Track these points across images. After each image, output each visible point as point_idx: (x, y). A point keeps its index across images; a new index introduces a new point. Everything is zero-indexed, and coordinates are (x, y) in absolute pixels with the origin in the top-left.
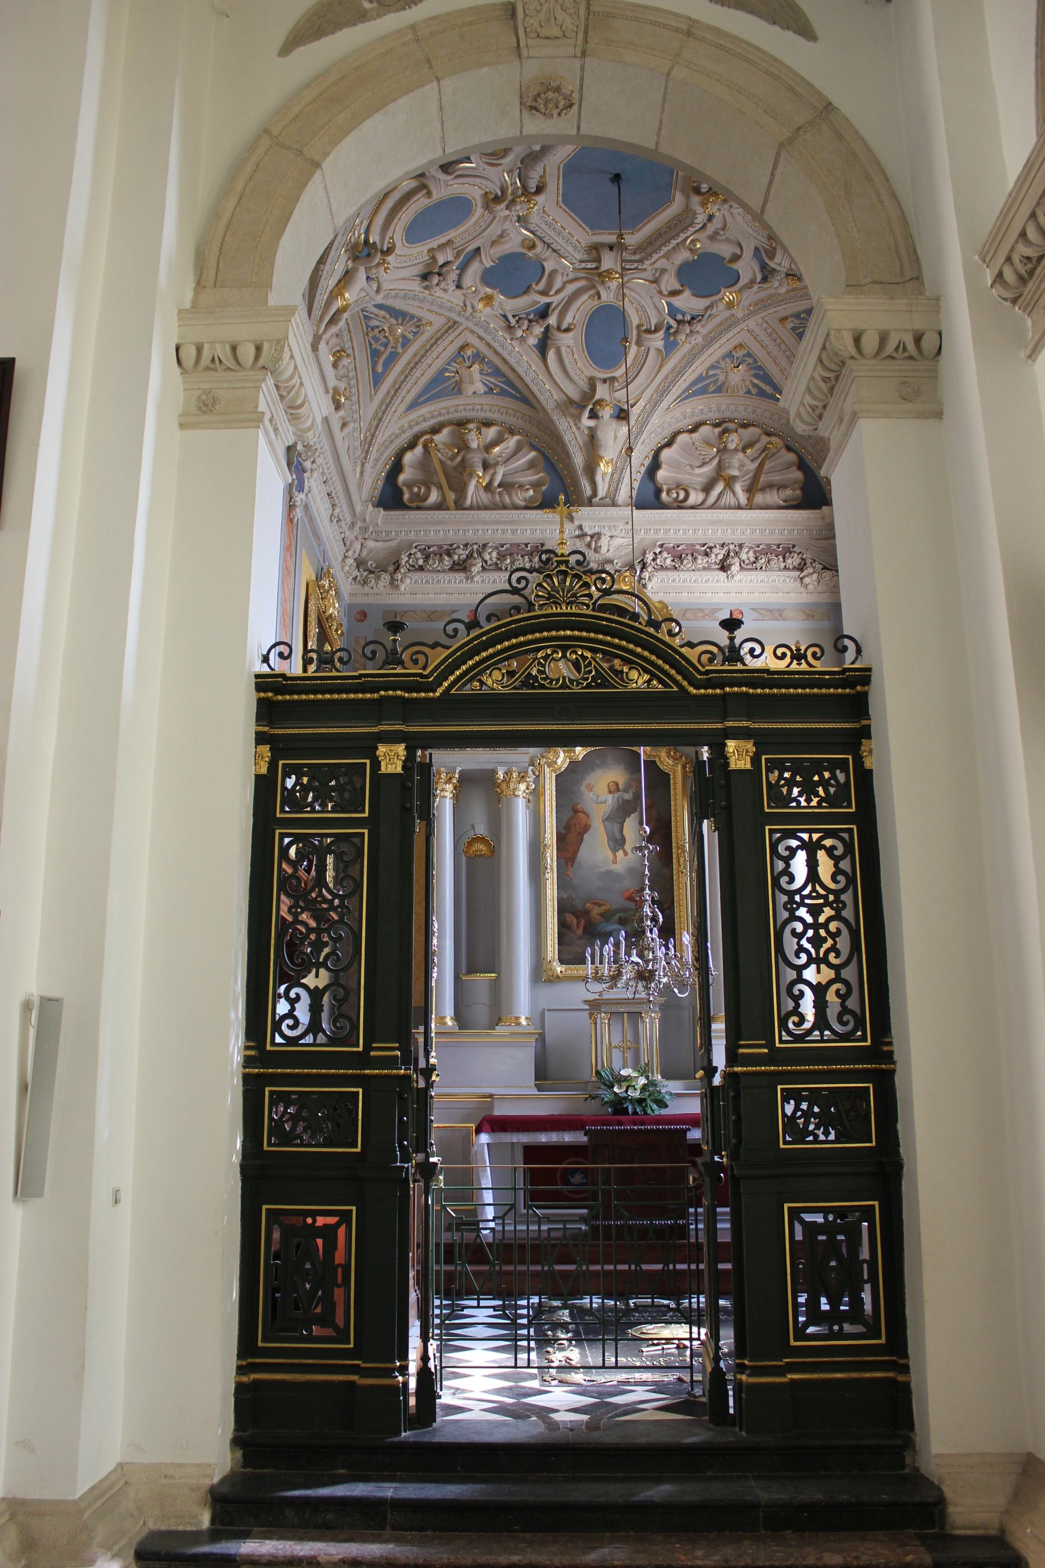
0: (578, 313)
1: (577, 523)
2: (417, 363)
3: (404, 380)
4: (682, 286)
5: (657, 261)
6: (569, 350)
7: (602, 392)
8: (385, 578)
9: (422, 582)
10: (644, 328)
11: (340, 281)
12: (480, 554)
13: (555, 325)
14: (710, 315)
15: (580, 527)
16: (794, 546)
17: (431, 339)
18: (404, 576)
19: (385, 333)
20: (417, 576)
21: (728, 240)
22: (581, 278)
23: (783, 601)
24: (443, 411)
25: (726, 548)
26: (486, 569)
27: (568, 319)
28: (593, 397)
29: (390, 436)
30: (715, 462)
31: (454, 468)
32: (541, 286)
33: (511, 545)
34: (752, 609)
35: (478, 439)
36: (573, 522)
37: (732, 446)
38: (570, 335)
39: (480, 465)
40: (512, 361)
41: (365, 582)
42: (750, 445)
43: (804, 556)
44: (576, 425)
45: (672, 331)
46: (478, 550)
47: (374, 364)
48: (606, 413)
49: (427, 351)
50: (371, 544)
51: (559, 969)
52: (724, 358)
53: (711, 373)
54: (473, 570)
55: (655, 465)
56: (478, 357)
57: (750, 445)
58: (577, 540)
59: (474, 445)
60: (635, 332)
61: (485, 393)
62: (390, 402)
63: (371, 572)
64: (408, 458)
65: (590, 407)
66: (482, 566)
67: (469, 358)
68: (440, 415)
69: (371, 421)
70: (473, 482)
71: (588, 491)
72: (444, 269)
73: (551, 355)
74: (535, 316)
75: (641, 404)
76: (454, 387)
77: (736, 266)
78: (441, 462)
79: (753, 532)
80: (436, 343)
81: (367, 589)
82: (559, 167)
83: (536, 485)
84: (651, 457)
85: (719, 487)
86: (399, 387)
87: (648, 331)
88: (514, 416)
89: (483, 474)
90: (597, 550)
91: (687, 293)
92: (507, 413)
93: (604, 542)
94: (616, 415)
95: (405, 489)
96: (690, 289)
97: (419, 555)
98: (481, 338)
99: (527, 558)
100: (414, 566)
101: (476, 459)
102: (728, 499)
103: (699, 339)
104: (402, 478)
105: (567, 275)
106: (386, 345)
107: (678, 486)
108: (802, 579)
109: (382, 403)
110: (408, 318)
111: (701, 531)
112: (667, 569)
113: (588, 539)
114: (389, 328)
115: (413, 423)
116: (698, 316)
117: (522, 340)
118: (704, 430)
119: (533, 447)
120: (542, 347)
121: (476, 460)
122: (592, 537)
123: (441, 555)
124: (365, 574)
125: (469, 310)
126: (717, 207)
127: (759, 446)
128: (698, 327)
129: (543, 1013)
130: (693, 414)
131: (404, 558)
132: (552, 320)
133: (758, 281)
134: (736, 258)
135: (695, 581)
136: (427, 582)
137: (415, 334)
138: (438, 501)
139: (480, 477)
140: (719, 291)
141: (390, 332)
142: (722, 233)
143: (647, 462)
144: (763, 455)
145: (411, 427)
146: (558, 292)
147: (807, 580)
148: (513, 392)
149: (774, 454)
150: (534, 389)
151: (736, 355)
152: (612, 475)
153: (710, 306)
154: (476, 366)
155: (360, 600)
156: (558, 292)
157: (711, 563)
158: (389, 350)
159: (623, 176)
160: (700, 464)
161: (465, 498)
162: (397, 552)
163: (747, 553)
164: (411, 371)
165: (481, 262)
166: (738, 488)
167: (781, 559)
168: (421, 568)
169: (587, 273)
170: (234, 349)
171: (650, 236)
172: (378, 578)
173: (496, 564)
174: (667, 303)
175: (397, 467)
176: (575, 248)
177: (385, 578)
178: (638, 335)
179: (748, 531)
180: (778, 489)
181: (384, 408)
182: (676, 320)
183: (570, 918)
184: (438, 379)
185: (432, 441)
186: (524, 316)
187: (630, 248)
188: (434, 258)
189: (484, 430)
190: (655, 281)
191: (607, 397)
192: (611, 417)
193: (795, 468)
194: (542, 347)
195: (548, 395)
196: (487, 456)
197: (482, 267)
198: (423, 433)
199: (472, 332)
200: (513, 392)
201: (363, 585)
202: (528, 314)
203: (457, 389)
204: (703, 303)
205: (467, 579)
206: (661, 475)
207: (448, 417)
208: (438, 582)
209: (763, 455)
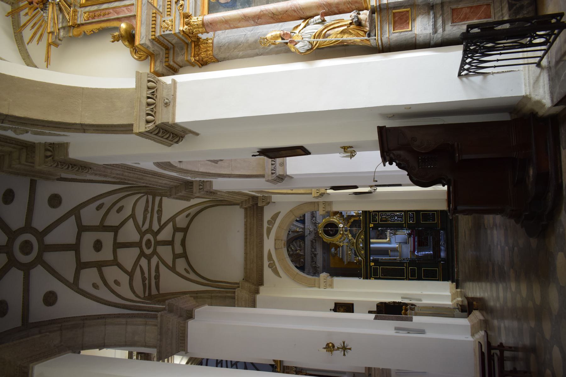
12: (313, 252)
18: (317, 265)
20: (317, 263)
50: (311, 272)
51: (388, 239)
71: (301, 233)
83: (300, 242)
90: (312, 231)
93: (311, 230)
95: (300, 265)
104: (298, 266)
119: (293, 242)
121: (295, 253)
129: (396, 243)
168: (315, 262)
170: (324, 282)
172: (318, 270)
183: (379, 238)
189: (289, 251)
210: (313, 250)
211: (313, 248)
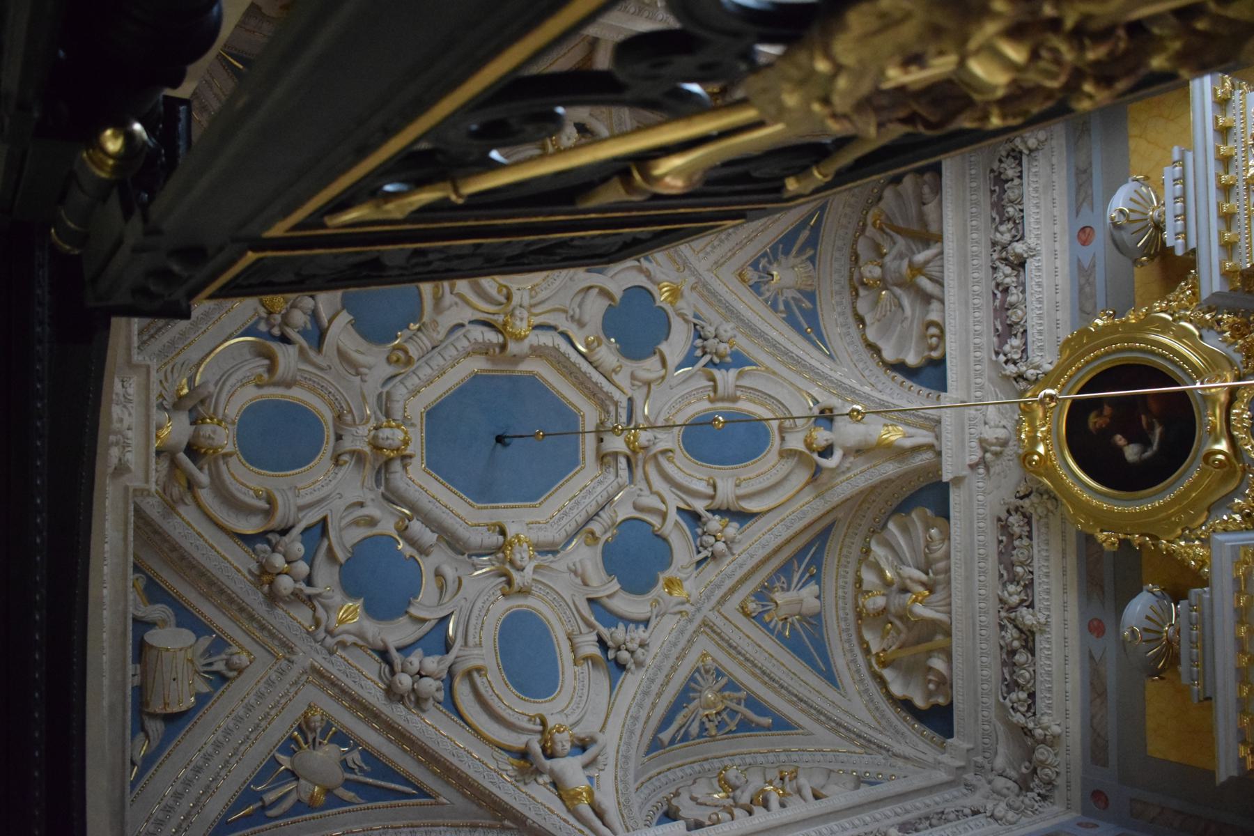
0: (695, 476)
1: (966, 472)
2: (764, 673)
3: (786, 689)
4: (655, 353)
5: (621, 388)
6: (743, 484)
7: (795, 442)
9: (1049, 698)
10: (712, 394)
11: (560, 797)
12: (1012, 609)
13: (706, 503)
14: (696, 316)
15: (973, 467)
16: (992, 171)
17: (730, 654)
18: (1037, 724)
19: (711, 715)
20: (1041, 705)
21: (580, 306)
22: (645, 473)
23: (1064, 173)
24: (844, 636)
25: (998, 263)
26: (1033, 601)
27: (702, 487)
28: (801, 453)
29: (869, 710)
30: (898, 291)
31: (910, 629)
32: (655, 521)
33: (1000, 563)
34: (1077, 216)
35: (873, 595)
36: (963, 478)
37: (877, 271)
38: (720, 484)
39: (902, 596)
40: (761, 554)
41: (1050, 783)
42: (877, 248)
43: (1004, 153)
44: (843, 473)
45: (716, 360)
46: (1007, 611)
47: (760, 727)
48: (822, 436)
49: (747, 660)
50: (1000, 762)
52: (760, 294)
53: (782, 307)
54: (1028, 622)
55: (900, 368)
56: (763, 594)
57: (877, 248)
58: (992, 471)
59: (880, 601)
60: (719, 405)
61: (818, 583)
62: (815, 709)
63: (1034, 771)
64: (897, 689)
65: (815, 456)
66: (1028, 607)
67: (763, 606)
68: (849, 641)
69: (841, 737)
70: (919, 609)
71: (925, 458)
72: (610, 643)
73: (751, 506)
74: (699, 527)
75: (815, 391)
76: (809, 623)
77: (618, 295)
79: (976, 229)
80: (735, 648)
81: (1060, 782)
82: (479, 508)
84: (894, 374)
85: (924, 282)
86: (796, 696)
87: (715, 389)
88: (850, 547)
89: (914, 594)
90: (1004, 444)
91: (664, 347)
92: (846, 557)
94: (828, 423)
95: (933, 700)
96: (659, 343)
97: (1013, 696)
98: (732, 590)
99: (1017, 543)
100: (1029, 707)
101: (896, 602)
102: (932, 269)
103: (727, 329)
104: (920, 702)
105: (641, 490)
106: (733, 713)
107: (924, 337)
108: (1031, 151)
109: (818, 720)
110: (693, 685)
111: (976, 301)
112: (1025, 344)
113: (988, 455)
114: (704, 709)
115: (856, 677)
116: (695, 329)
117: (729, 543)
118: (862, 307)
119: (884, 526)
120: (743, 517)
121: (898, 601)
122: (985, 451)
123: (1014, 664)
124: (1036, 780)
125: (687, 607)
126: (518, 323)
127: (879, 238)
128: (710, 330)
130: (844, 325)
131: (1018, 718)
132: (700, 506)
133: (637, 263)
134: (604, 293)
135: (1040, 302)
136: (1049, 690)
137: (719, 673)
138: (945, 658)
139: (915, 601)
140: (661, 307)
141: (710, 708)
142: (571, 313)
143: (899, 378)
144: (888, 230)
145: (862, 681)
146: (664, 502)
147: (1032, 143)
148: (814, 549)
149: (887, 217)
150: (799, 526)
151: (756, 279)
152: (907, 424)
153: (683, 316)
154: (779, 597)
155: (1076, 795)
156: (664, 502)
157: (1017, 282)
158: (742, 708)
159: (500, 433)
160: (900, 310)
161: (941, 621)
163: (1002, 234)
164: (774, 680)
165: (609, 596)
166: (920, 257)
167: (1009, 184)
168: (1032, 695)
169: (637, 466)
171: (586, 396)
173: (1025, 586)
174: (677, 369)
175: (906, 705)
176: (600, 482)
177: (1042, 753)
178: (722, 400)
179: (974, 236)
180: (924, 204)
181: (822, 718)
182: (703, 356)
184: (794, 645)
185: (877, 654)
186: (699, 540)
187: (603, 418)
188: (586, 659)
189: (864, 588)
190: (648, 384)
191: (801, 436)
192: (830, 429)
193: (899, 188)
194: (743, 517)
195: (809, 508)
196: (895, 587)
197: (622, 594)
198: (870, 666)
199: (723, 600)
200: (814, 549)
201: (1053, 786)
202: (695, 536)
203: (814, 621)
204: (677, 323)
205: (1045, 631)
206: (912, 359)
207: (853, 631)
208: (1049, 674)
209: (888, 230)
210: (1014, 594)
211: (1014, 579)
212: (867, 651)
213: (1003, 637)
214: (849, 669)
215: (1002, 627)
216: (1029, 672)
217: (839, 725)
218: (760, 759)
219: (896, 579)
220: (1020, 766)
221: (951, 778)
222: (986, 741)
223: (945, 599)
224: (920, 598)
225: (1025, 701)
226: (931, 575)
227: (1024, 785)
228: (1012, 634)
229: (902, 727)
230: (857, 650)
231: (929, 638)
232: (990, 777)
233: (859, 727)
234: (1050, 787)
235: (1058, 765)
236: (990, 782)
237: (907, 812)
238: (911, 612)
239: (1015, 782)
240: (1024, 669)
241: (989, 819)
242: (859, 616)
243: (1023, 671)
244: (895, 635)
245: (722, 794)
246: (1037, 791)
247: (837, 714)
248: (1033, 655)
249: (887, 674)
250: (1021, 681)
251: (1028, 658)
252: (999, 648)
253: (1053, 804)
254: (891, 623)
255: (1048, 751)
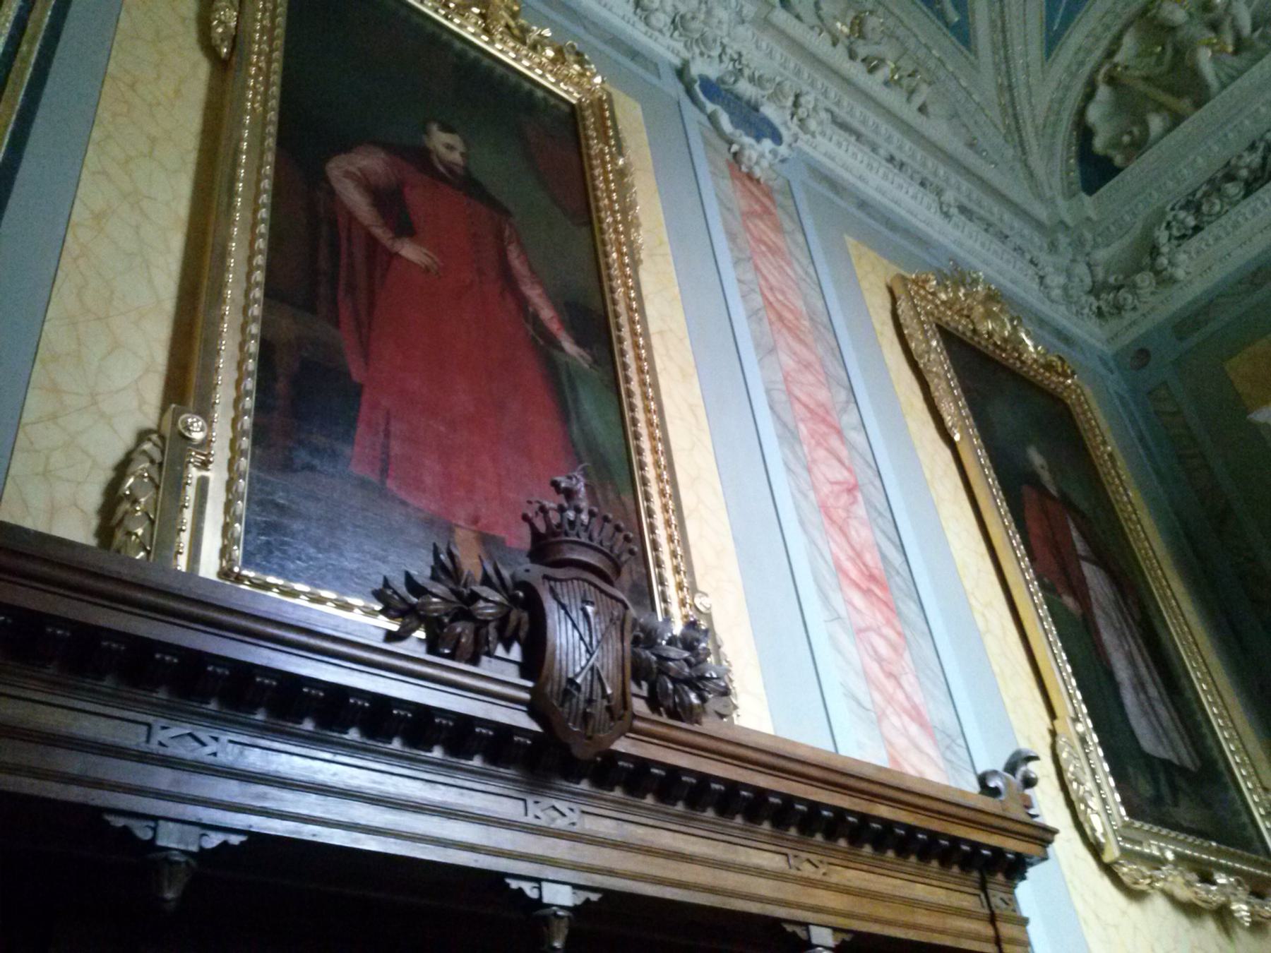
8: (1145, 280)
9: (1207, 245)
20: (1194, 243)
41: (1118, 308)
47: (941, 15)
64: (1094, 114)
70: (1204, 57)
78: (1147, 79)
81: (1128, 316)
95: (1111, 153)
97: (1182, 215)
104: (1099, 144)
115: (1074, 68)
123: (1219, 190)
124: (1112, 295)
131: (1162, 235)
136: (1217, 239)
161: (1208, 87)
162: (1148, 232)
168: (1197, 229)
172: (1134, 288)
175: (1084, 133)
177: (1145, 280)
181: (1003, 67)
185: (1116, 66)
196: (1211, 15)
198: (1096, 71)
201: (1120, 313)
212: (1110, 54)
213: (1240, 157)
214: (1076, 53)
215: (1252, 147)
216: (1222, 207)
217: (1010, 88)
218: (911, 43)
219: (1220, 11)
220: (1114, 273)
221: (1047, 222)
222: (1113, 229)
223: (1237, 70)
224: (1217, 48)
225: (1186, 229)
226: (1257, 34)
227: (1095, 291)
228: (1251, 161)
229: (1060, 148)
230: (1104, 43)
231: (1178, 94)
232: (1079, 258)
233: (1026, 112)
234: (1115, 311)
235: (1145, 302)
236: (1074, 261)
237: (980, 205)
238: (1194, 51)
239: (1094, 282)
240: (1221, 200)
241: (1037, 277)
242: (1144, 12)
243: (1217, 201)
244: (1152, 63)
245: (846, 30)
246: (1102, 303)
247: (1020, 77)
248: (1246, 196)
249: (1103, 92)
250: (1205, 208)
251: (1237, 195)
252: (1224, 163)
253: (1101, 326)
254: (1163, 49)
255: (1150, 284)
